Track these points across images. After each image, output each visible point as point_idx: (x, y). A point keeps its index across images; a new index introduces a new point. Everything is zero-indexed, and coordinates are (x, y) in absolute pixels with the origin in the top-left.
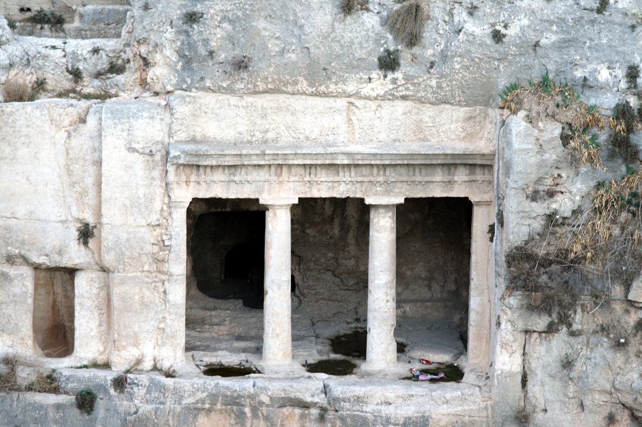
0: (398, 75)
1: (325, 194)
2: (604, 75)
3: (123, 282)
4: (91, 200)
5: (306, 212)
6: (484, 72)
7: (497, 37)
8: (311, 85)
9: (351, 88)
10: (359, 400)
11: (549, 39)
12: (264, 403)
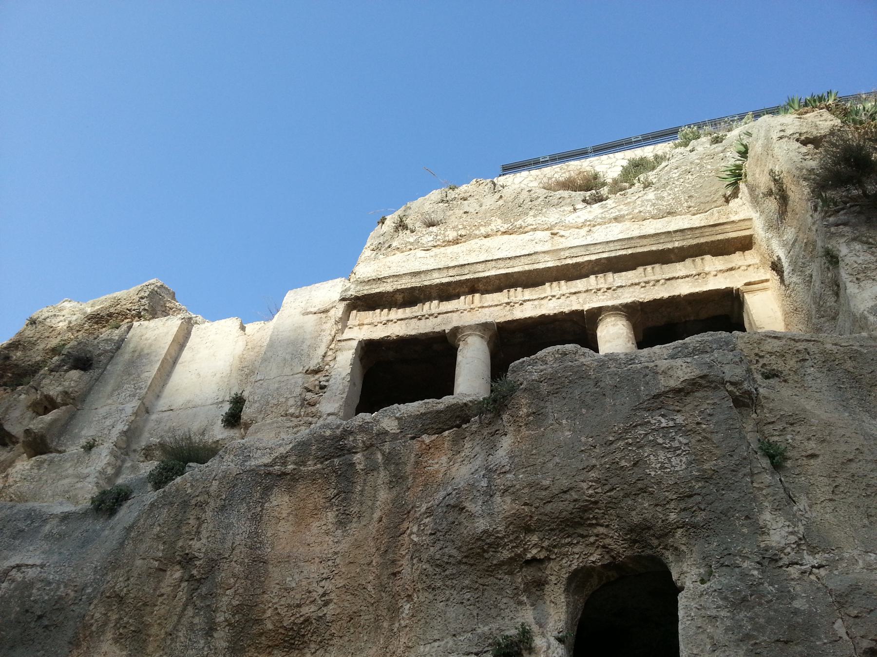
6: (709, 167)
12: (386, 433)
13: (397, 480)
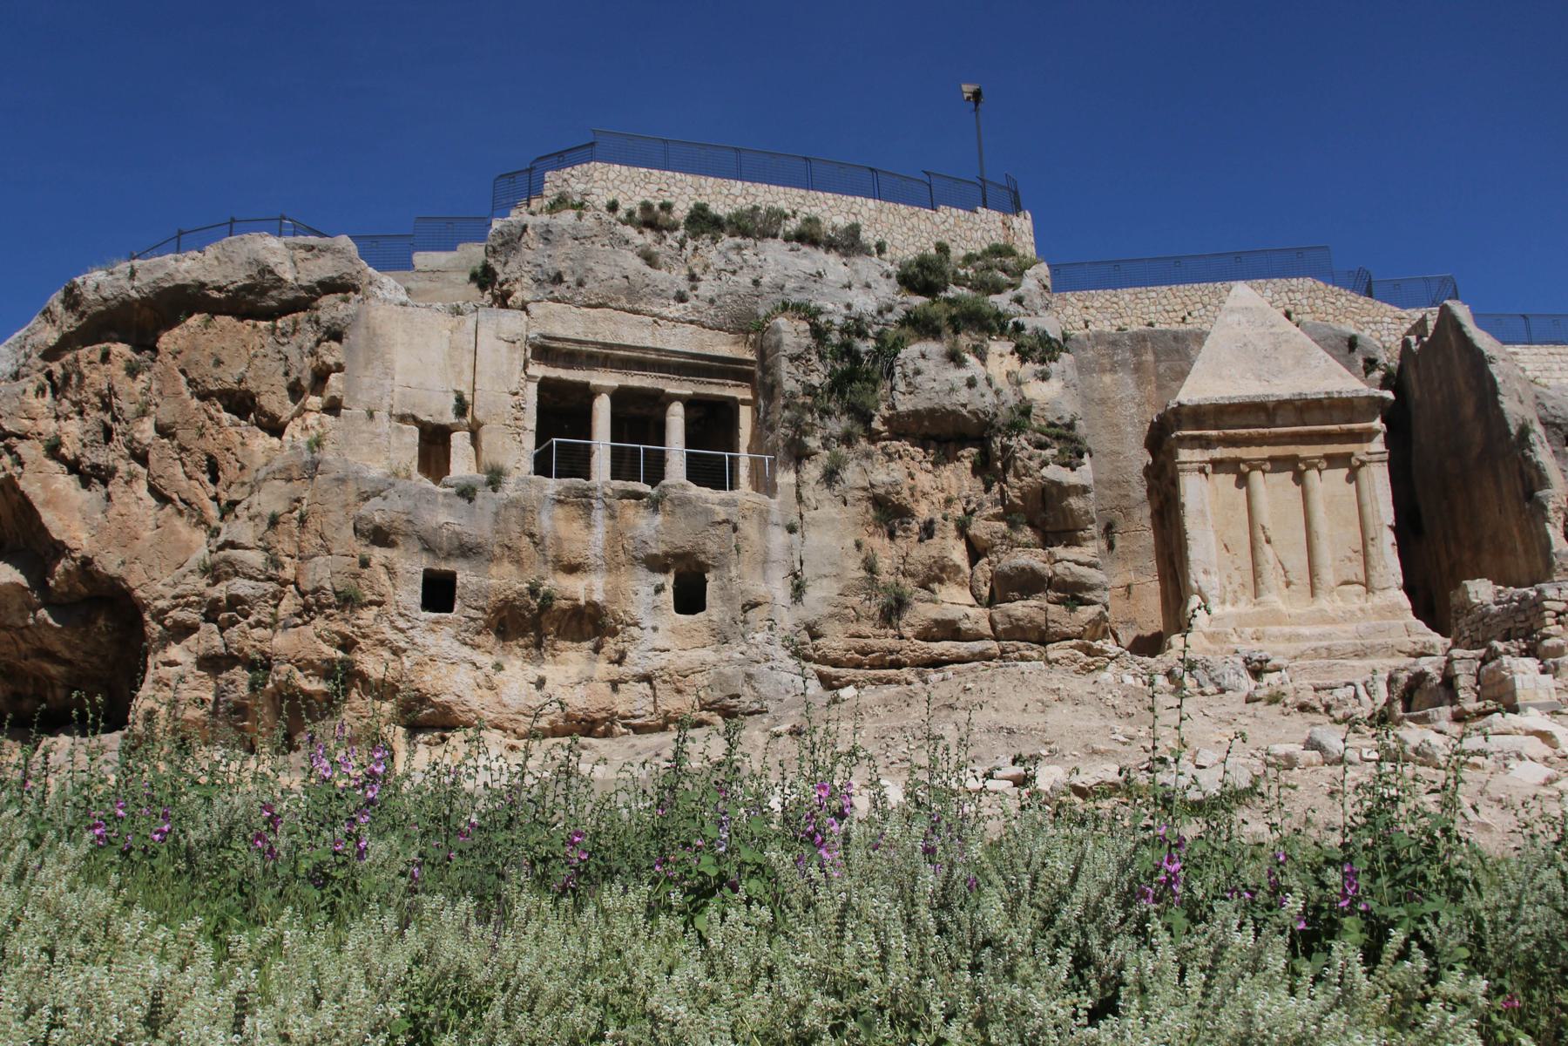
2: (830, 307)
3: (490, 432)
4: (468, 375)
5: (621, 397)
7: (756, 283)
9: (656, 310)
11: (790, 285)
13: (612, 517)
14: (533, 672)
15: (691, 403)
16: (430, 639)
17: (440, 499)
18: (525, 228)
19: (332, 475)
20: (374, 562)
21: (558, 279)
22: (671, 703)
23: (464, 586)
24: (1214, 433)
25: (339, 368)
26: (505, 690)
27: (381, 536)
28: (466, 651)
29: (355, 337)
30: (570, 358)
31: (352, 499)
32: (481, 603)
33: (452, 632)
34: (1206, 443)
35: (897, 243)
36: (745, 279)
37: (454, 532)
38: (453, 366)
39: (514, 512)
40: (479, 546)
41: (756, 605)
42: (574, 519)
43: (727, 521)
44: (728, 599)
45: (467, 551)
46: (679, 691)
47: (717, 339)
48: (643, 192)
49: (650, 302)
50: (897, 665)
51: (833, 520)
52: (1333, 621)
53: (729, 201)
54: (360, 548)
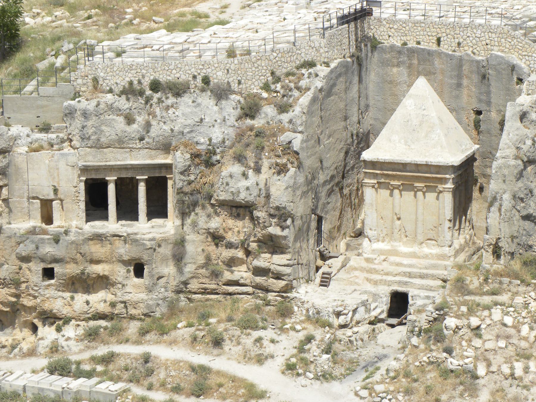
0: (144, 142)
1: (124, 176)
2: (202, 140)
3: (66, 203)
7: (172, 130)
8: (119, 145)
9: (131, 146)
10: (136, 234)
14: (85, 297)
15: (147, 181)
16: (47, 292)
17: (46, 241)
18: (76, 110)
19: (6, 235)
20: (23, 267)
21: (89, 138)
22: (132, 311)
23: (57, 273)
24: (378, 172)
25: (6, 185)
26: (75, 306)
27: (26, 259)
28: (60, 293)
29: (11, 170)
30: (97, 169)
31: (14, 244)
32: (64, 278)
33: (54, 288)
34: (375, 176)
35: (248, 77)
36: (166, 127)
37: (52, 255)
38: (51, 175)
39: (74, 245)
40: (61, 259)
41: (163, 277)
42: (97, 244)
43: (151, 248)
44: (151, 276)
45: (56, 261)
46: (135, 308)
47: (158, 153)
48: (130, 75)
49: (129, 144)
50: (217, 294)
51: (194, 241)
52: (419, 257)
53: (168, 73)
54: (18, 262)
